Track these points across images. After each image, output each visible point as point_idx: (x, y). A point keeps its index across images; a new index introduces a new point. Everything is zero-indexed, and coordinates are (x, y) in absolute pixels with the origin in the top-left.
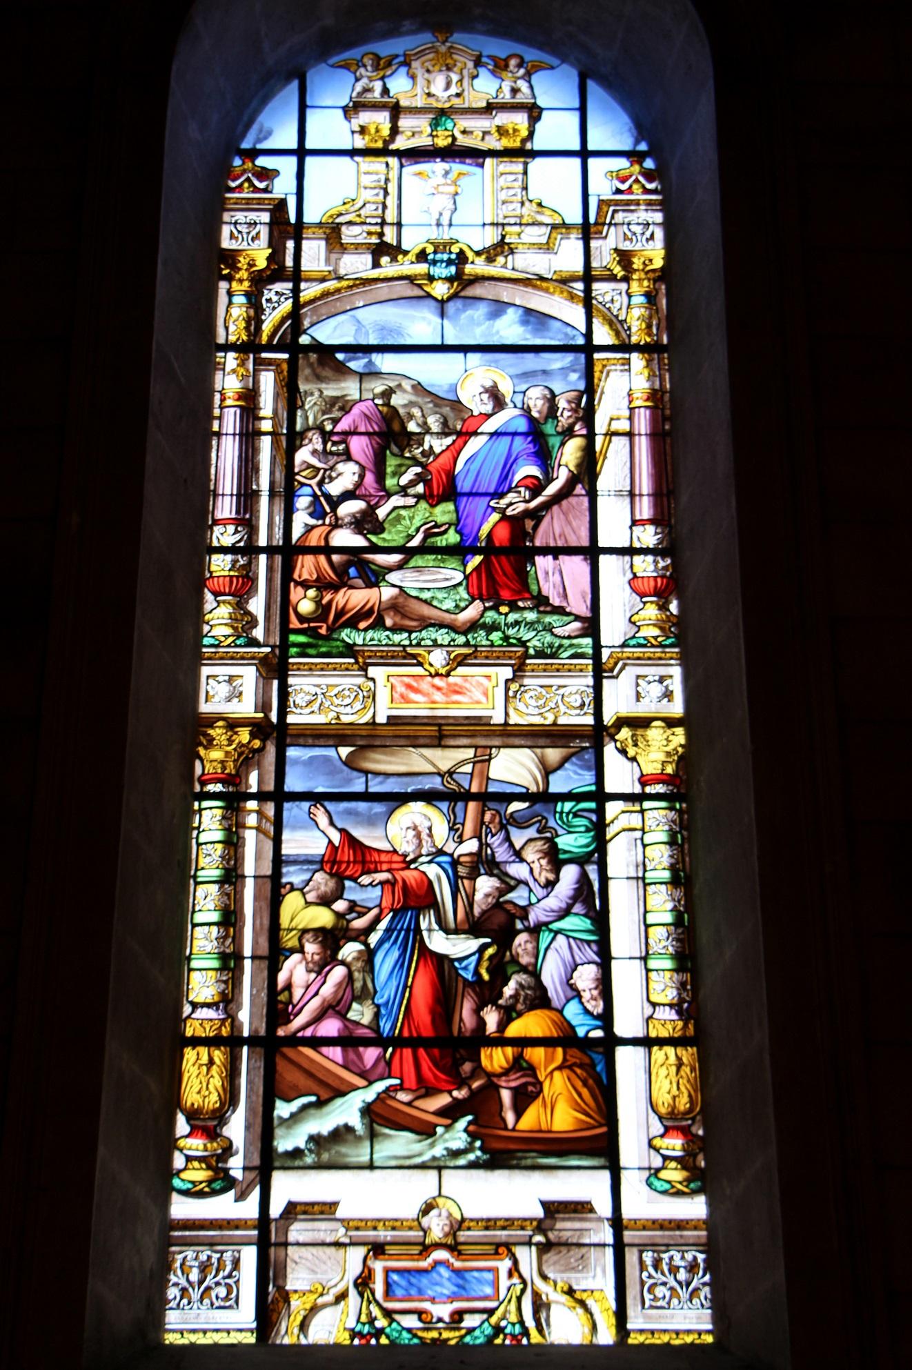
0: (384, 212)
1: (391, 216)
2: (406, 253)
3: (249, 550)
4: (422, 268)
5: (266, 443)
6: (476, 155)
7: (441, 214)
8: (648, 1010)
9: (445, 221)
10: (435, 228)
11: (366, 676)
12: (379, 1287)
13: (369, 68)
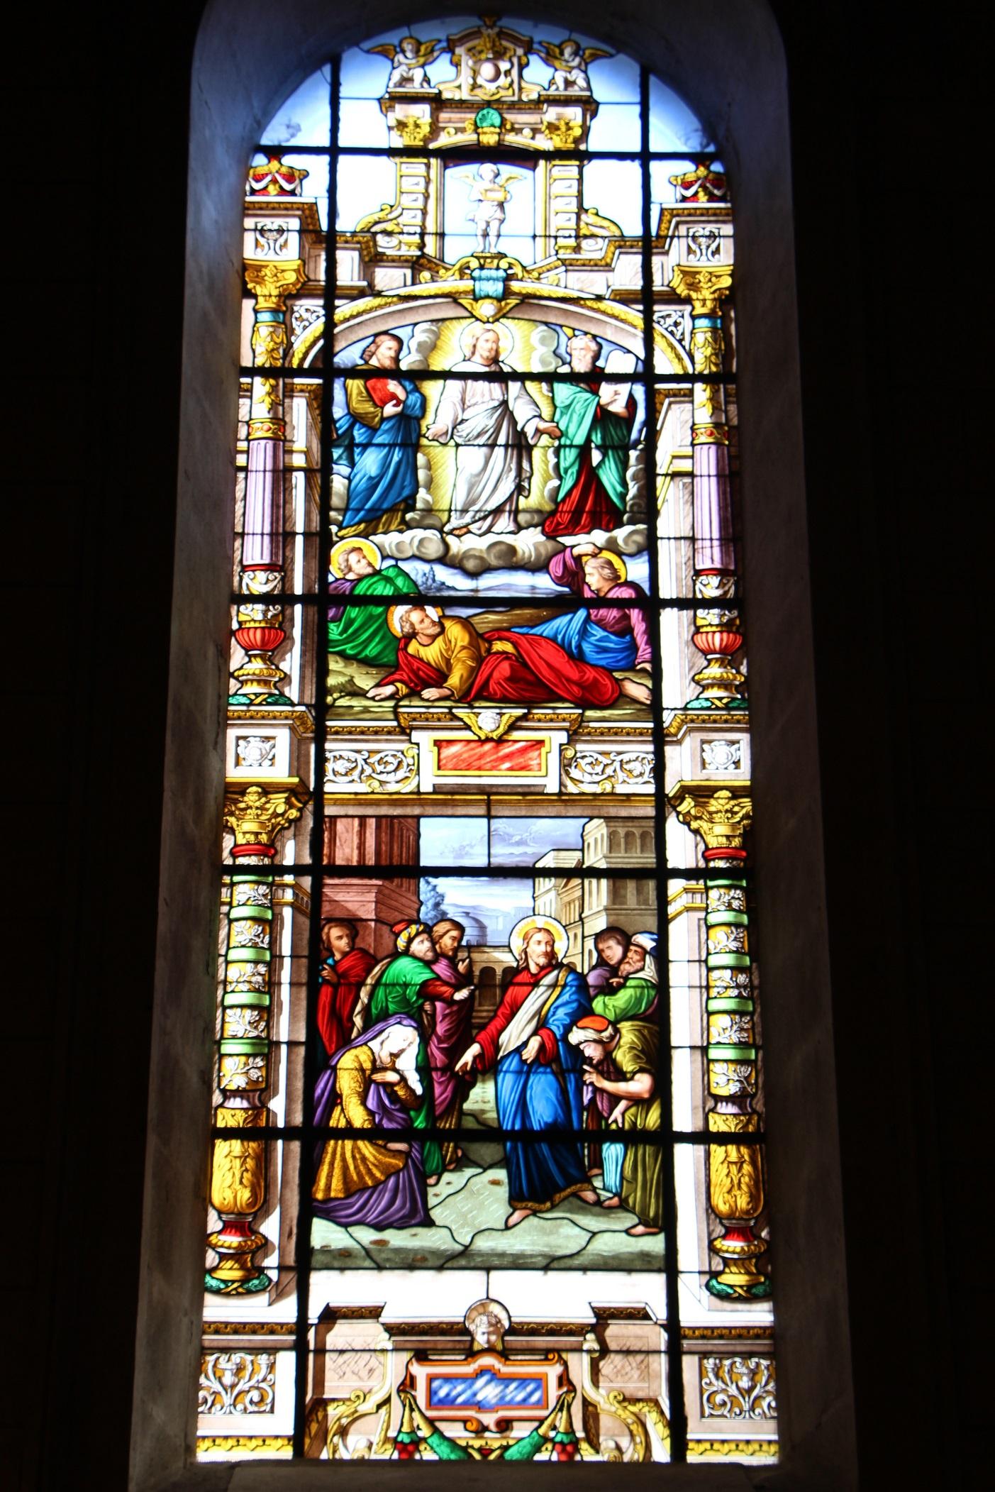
1: (431, 227)
3: (283, 598)
4: (467, 285)
5: (299, 479)
6: (527, 158)
7: (488, 224)
8: (711, 1104)
9: (493, 231)
10: (480, 239)
12: (421, 1394)
13: (409, 55)
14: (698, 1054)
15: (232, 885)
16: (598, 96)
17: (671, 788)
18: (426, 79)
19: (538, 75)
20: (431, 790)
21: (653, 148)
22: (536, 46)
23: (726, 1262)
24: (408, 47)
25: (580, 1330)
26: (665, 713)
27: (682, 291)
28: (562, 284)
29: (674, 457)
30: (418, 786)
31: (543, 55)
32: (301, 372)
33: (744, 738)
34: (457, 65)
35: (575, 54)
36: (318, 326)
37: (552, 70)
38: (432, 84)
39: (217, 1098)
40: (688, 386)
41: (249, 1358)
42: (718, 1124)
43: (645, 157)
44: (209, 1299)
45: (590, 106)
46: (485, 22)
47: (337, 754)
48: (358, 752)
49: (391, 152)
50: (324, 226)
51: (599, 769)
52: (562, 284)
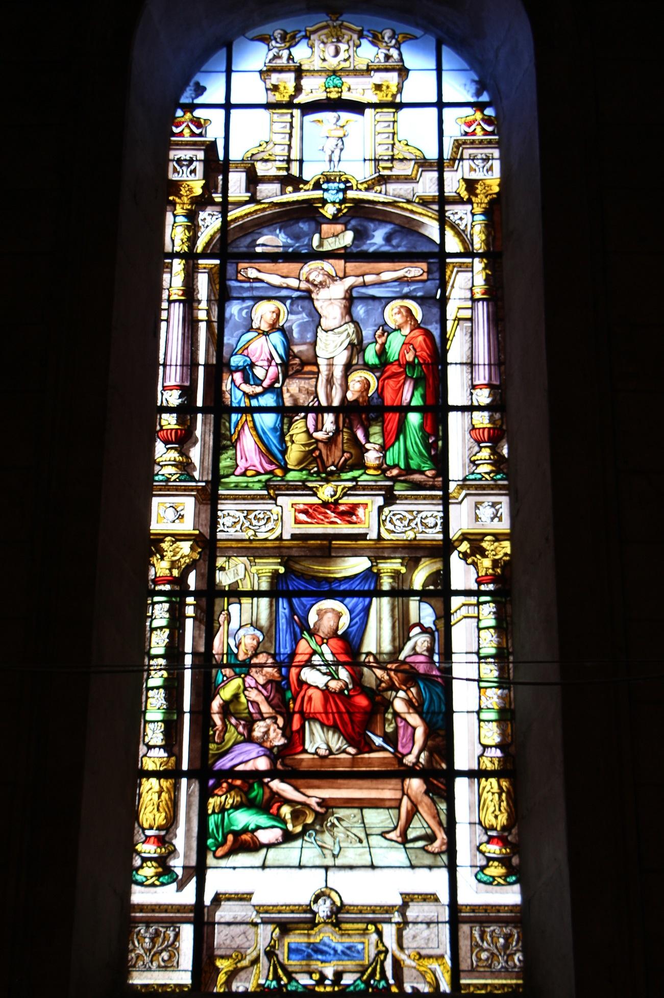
0: (289, 151)
1: (295, 155)
2: (306, 183)
4: (318, 194)
6: (357, 107)
7: (333, 152)
9: (335, 158)
11: (276, 504)
13: (278, 40)
14: (475, 715)
15: (154, 604)
16: (408, 65)
17: (454, 534)
18: (290, 58)
19: (368, 53)
20: (289, 537)
21: (445, 99)
22: (365, 33)
23: (489, 859)
25: (389, 909)
27: (465, 195)
28: (383, 192)
29: (459, 308)
30: (281, 534)
31: (370, 39)
32: (204, 255)
33: (505, 500)
34: (312, 47)
35: (391, 38)
37: (376, 49)
38: (295, 61)
39: (143, 749)
40: (470, 260)
41: (163, 930)
42: (487, 765)
43: (440, 105)
44: (135, 888)
45: (403, 72)
46: (331, 17)
47: (225, 512)
48: (242, 511)
49: (268, 106)
51: (406, 523)
52: (383, 192)
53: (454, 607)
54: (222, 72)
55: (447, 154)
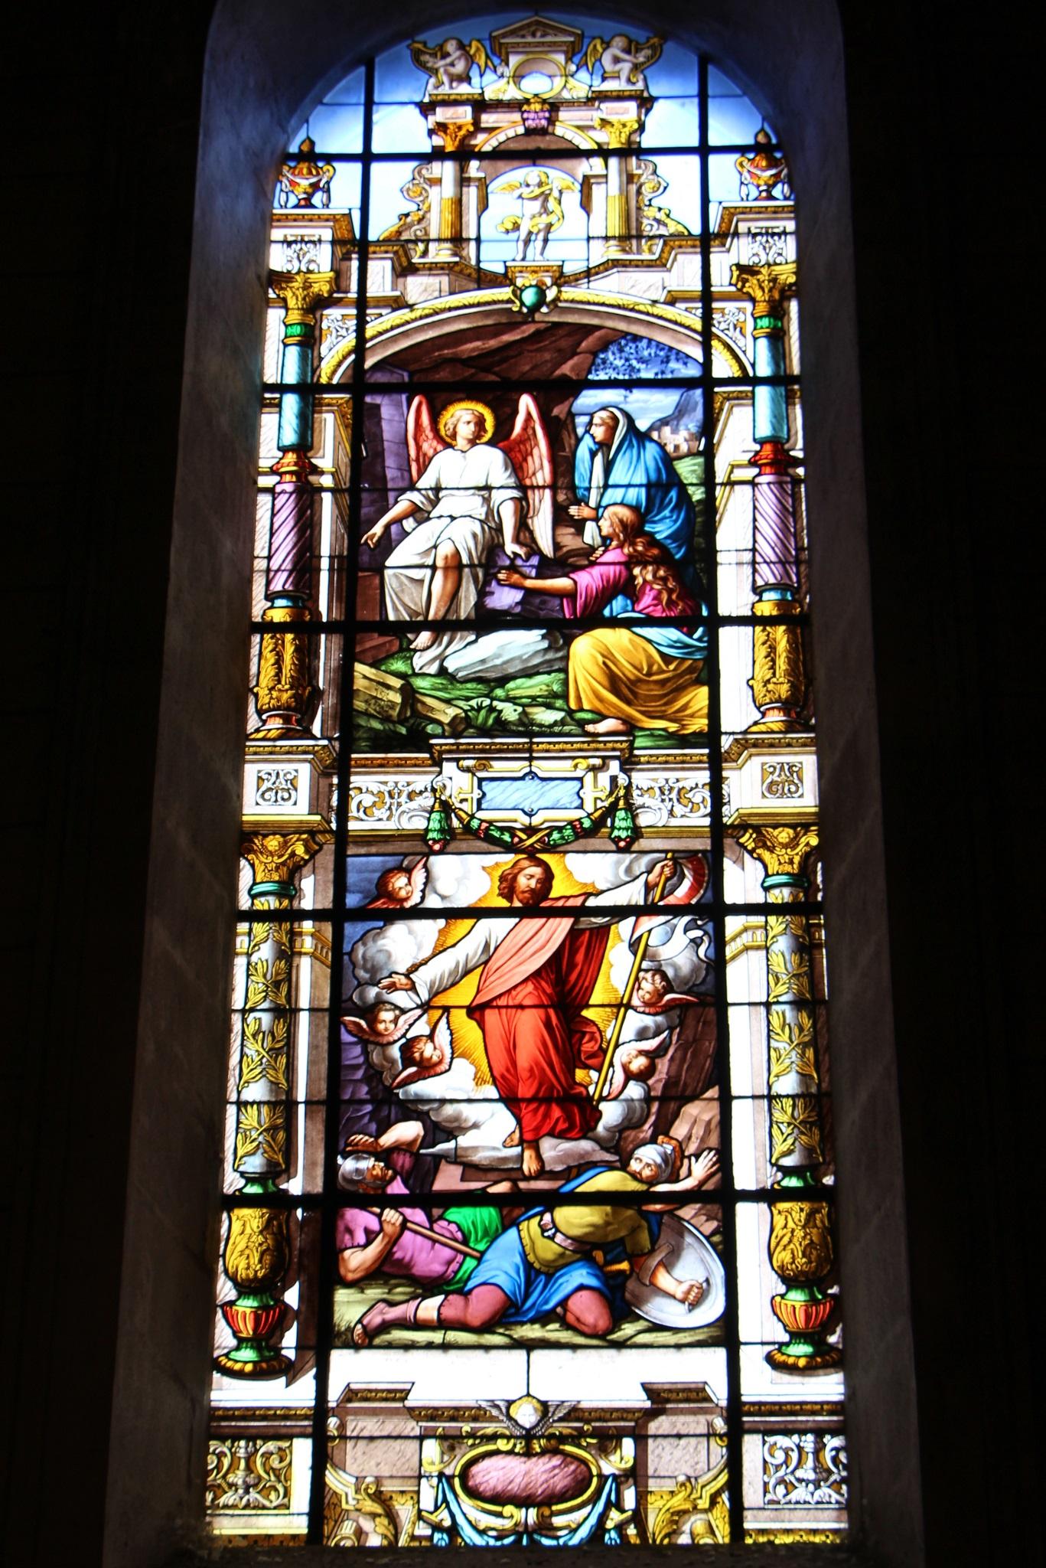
17: (729, 815)
24: (451, 47)
26: (724, 738)
36: (350, 341)
43: (704, 150)
45: (646, 102)
50: (358, 236)
53: (729, 933)
54: (358, 104)
55: (714, 226)
